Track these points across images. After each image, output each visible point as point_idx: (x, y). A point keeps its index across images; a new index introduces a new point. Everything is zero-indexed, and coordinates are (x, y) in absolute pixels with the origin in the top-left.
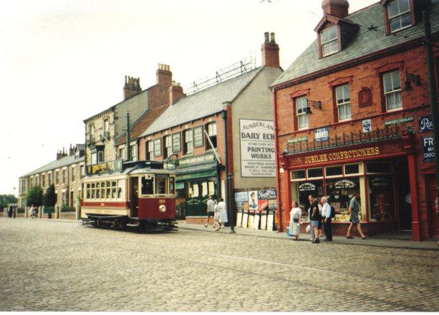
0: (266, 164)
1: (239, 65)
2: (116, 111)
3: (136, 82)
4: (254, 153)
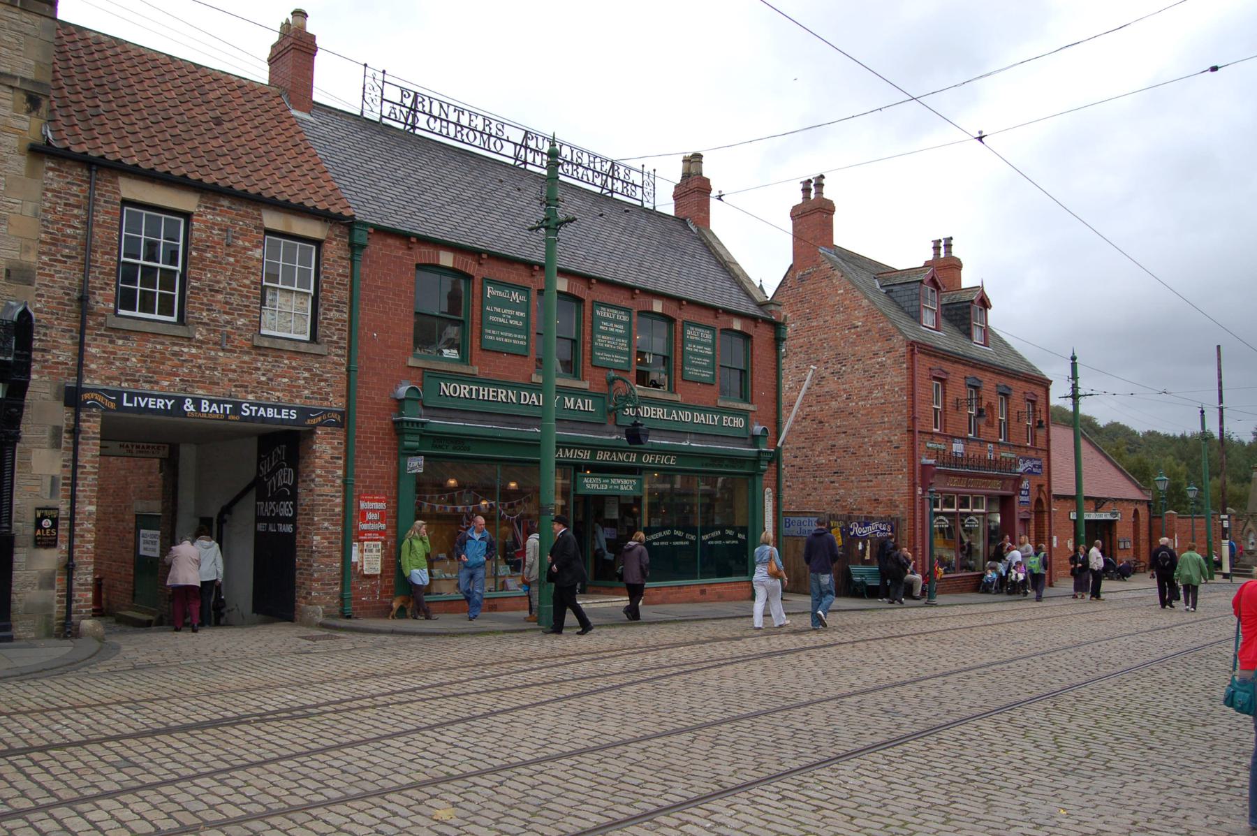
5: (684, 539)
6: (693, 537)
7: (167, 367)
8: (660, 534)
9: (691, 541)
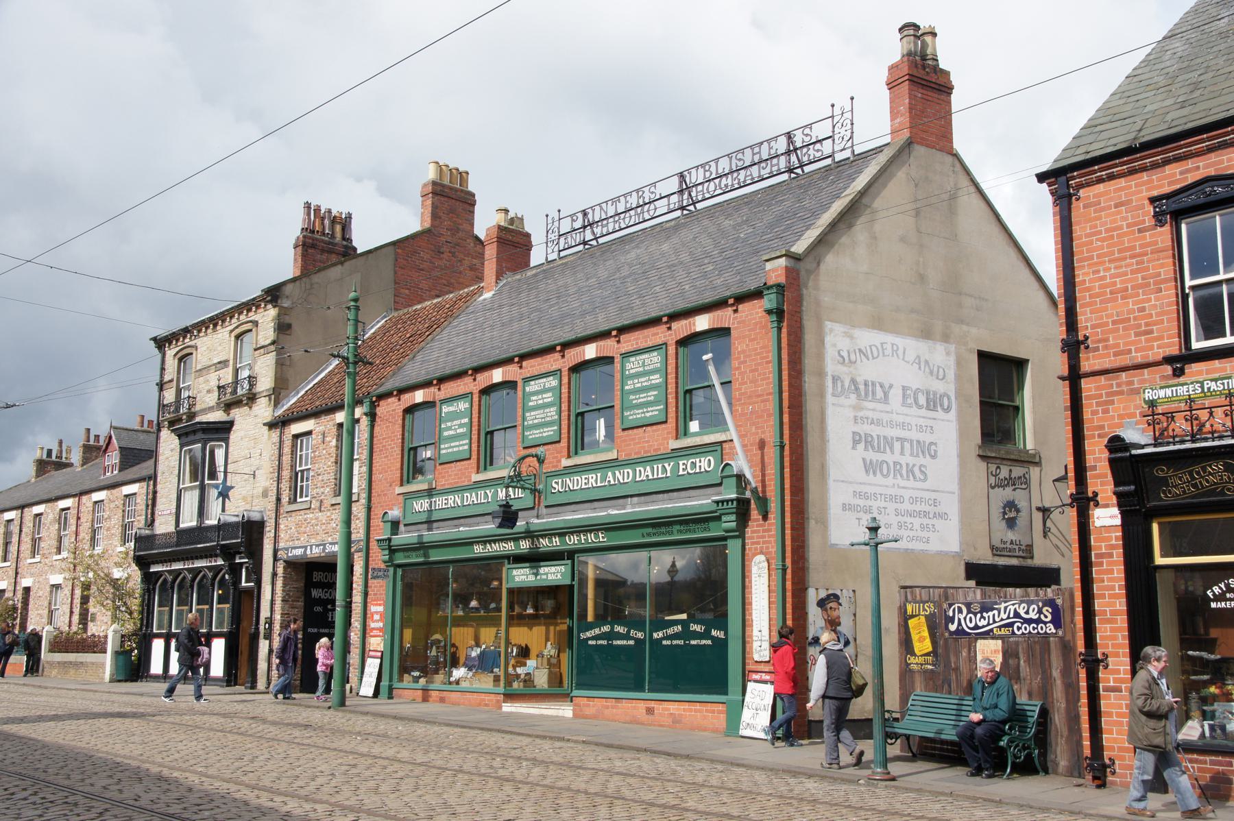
0: (914, 500)
1: (782, 145)
2: (286, 304)
3: (338, 228)
4: (872, 456)
5: (627, 637)
6: (640, 635)
7: (302, 529)
8: (597, 631)
9: (637, 640)
